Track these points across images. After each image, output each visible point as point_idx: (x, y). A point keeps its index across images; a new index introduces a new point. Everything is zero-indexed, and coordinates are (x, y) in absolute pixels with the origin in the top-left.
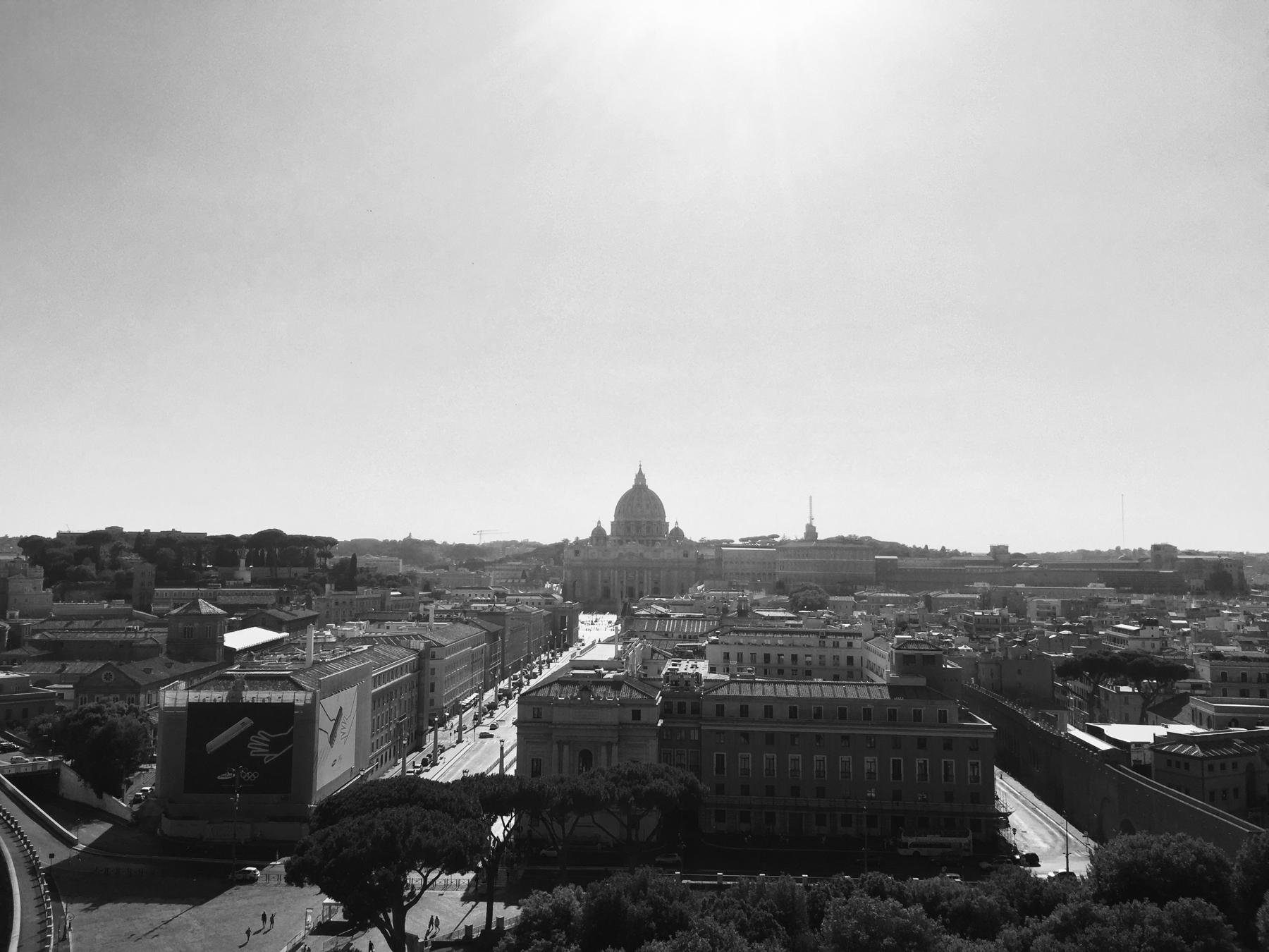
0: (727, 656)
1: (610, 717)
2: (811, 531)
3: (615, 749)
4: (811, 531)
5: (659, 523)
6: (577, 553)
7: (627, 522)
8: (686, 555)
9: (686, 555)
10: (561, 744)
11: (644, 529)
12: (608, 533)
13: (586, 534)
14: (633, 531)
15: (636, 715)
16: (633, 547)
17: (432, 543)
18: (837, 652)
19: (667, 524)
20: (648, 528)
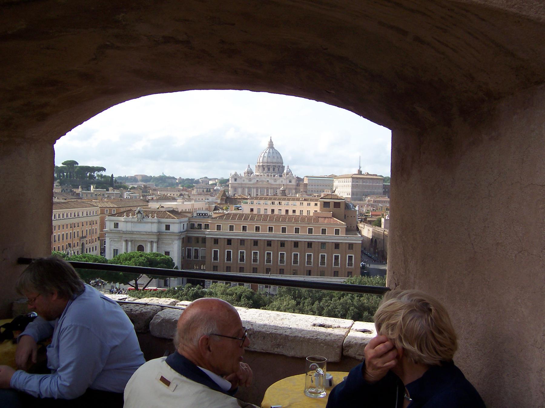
0: (252, 210)
1: (154, 228)
2: (360, 172)
3: (155, 245)
4: (360, 172)
5: (279, 166)
6: (236, 180)
7: (263, 166)
8: (290, 182)
9: (290, 182)
10: (126, 241)
11: (271, 169)
12: (254, 171)
13: (242, 172)
14: (266, 169)
15: (168, 227)
16: (265, 178)
17: (174, 178)
18: (309, 208)
19: (283, 167)
20: (274, 169)
